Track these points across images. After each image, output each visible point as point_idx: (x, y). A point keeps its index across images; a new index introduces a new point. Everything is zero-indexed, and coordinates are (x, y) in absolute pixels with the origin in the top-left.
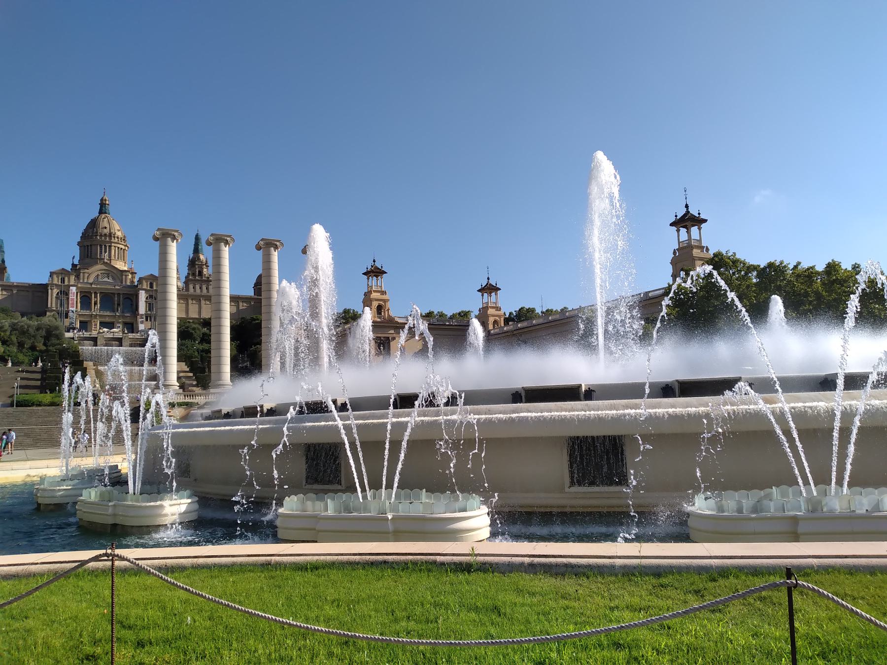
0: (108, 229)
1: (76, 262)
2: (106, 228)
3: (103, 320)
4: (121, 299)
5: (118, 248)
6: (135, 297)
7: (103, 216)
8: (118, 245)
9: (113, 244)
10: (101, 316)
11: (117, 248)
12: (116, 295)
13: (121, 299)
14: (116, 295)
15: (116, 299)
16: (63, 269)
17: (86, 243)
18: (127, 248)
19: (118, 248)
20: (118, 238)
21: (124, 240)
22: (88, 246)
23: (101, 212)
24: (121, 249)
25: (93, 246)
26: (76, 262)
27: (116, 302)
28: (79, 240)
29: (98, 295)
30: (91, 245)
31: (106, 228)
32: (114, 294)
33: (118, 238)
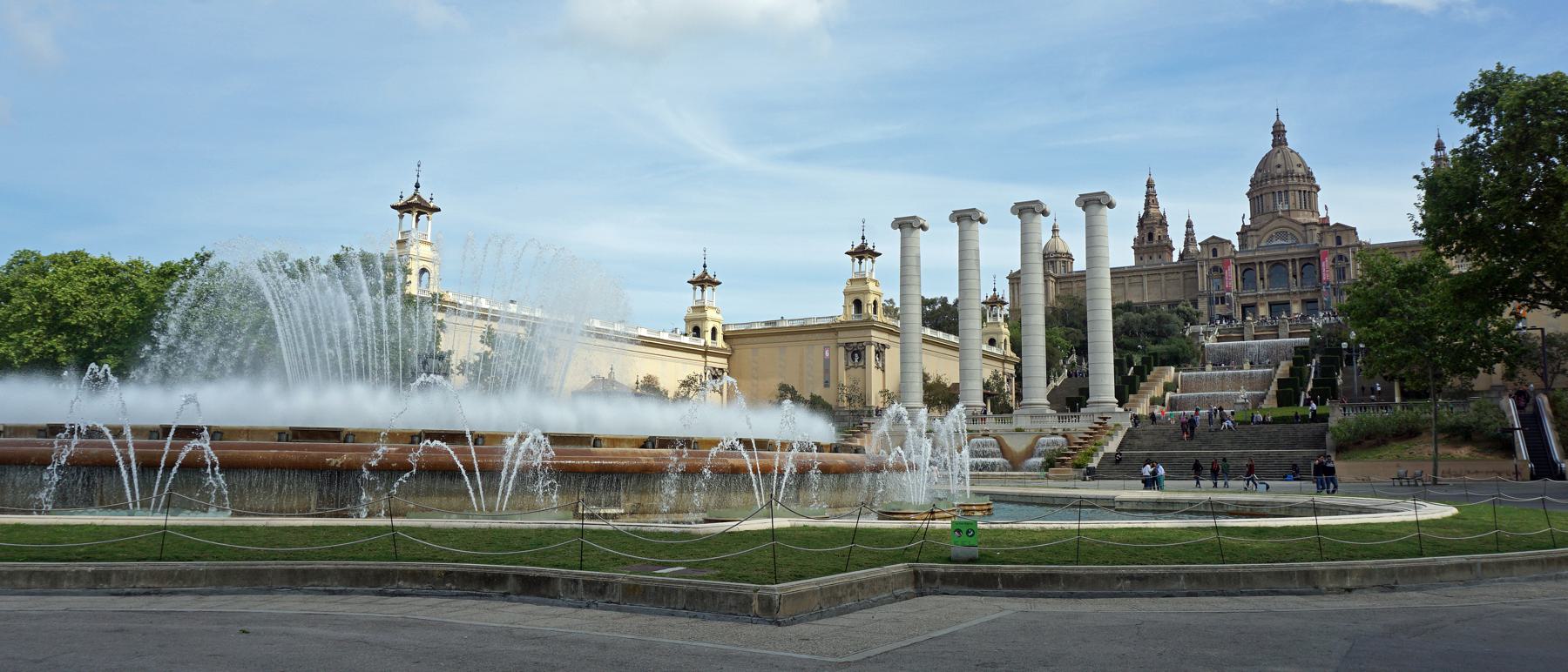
0: (1283, 166)
1: (1248, 222)
2: (1279, 166)
3: (1272, 299)
4: (1298, 267)
5: (1300, 191)
6: (1317, 261)
7: (1277, 149)
8: (1299, 188)
9: (1291, 188)
10: (1268, 295)
11: (1297, 193)
12: (1290, 263)
13: (1298, 267)
14: (1290, 263)
15: (1290, 268)
16: (1214, 237)
17: (1255, 194)
18: (1314, 190)
19: (1300, 191)
20: (1298, 177)
21: (1308, 178)
22: (1257, 197)
23: (1273, 145)
24: (1305, 192)
25: (1264, 197)
26: (1248, 222)
27: (1291, 273)
28: (1248, 189)
29: (1265, 266)
30: (1261, 195)
31: (1279, 166)
32: (1286, 261)
33: (1298, 177)
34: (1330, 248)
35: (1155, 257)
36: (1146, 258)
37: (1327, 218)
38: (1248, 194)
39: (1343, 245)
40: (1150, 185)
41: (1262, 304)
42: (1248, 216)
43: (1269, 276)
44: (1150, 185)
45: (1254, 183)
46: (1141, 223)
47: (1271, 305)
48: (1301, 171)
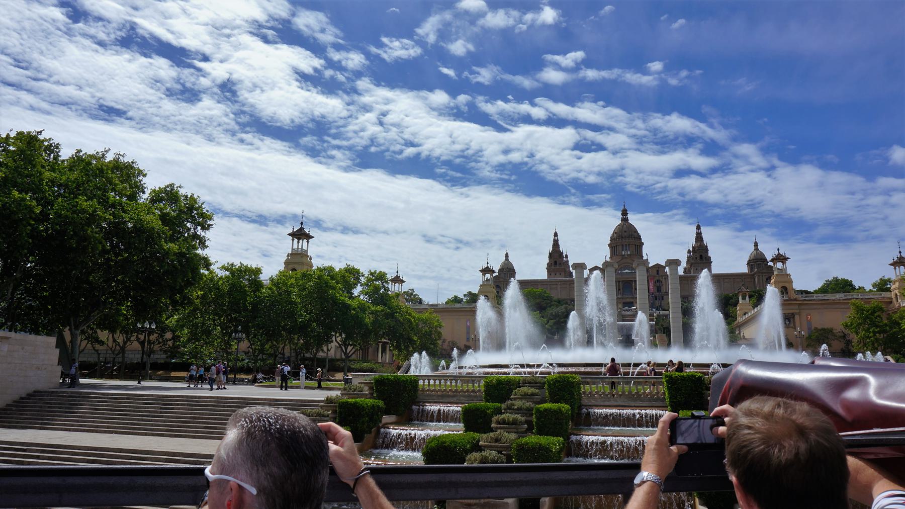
1: (608, 259)
2: (625, 232)
26: (608, 259)
31: (625, 232)
34: (654, 276)
35: (558, 274)
36: (553, 274)
37: (647, 259)
38: (609, 245)
39: (661, 274)
40: (556, 235)
41: (620, 303)
42: (609, 256)
43: (623, 289)
44: (556, 235)
45: (612, 239)
46: (551, 255)
47: (624, 303)
48: (635, 235)
